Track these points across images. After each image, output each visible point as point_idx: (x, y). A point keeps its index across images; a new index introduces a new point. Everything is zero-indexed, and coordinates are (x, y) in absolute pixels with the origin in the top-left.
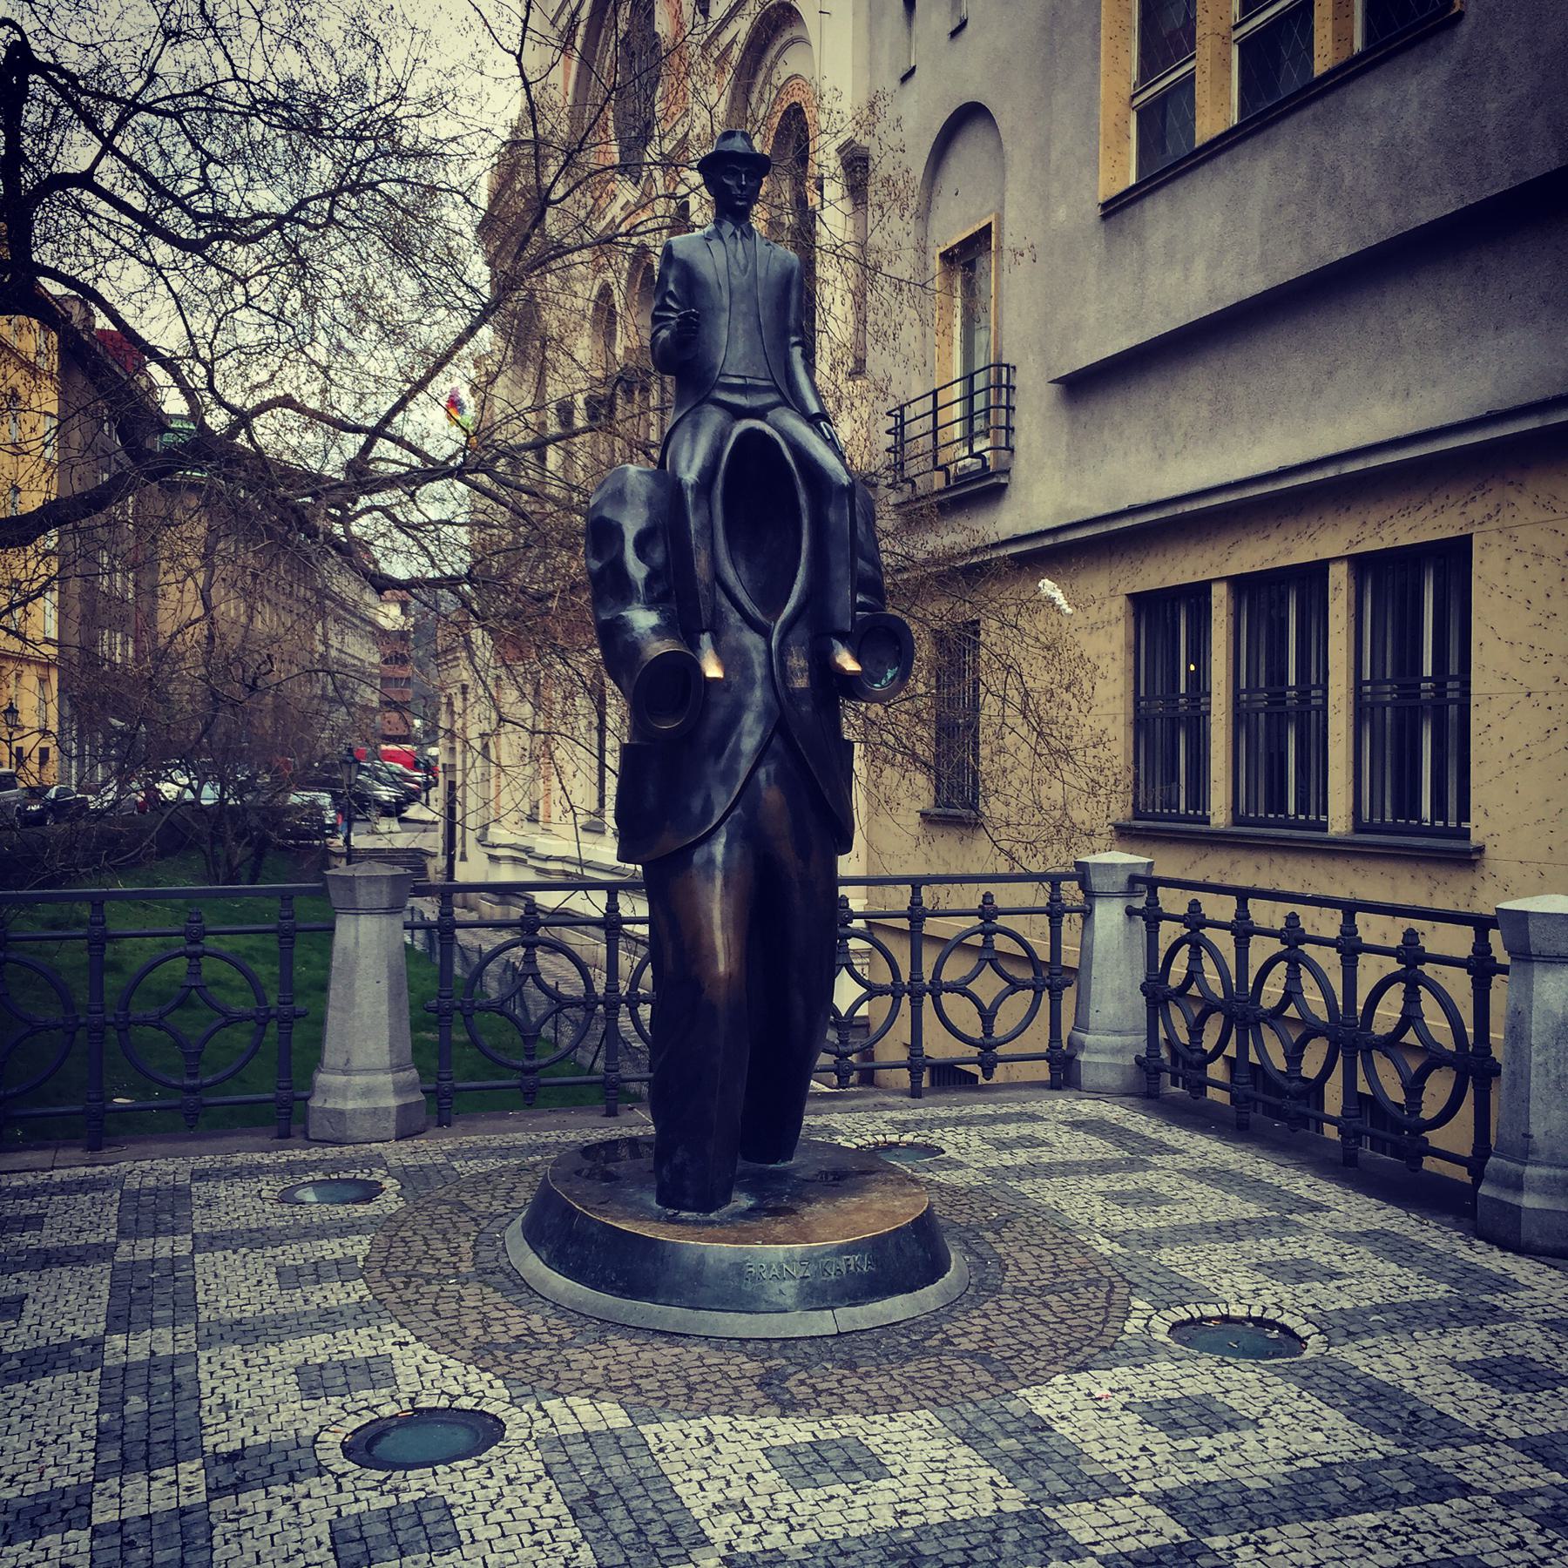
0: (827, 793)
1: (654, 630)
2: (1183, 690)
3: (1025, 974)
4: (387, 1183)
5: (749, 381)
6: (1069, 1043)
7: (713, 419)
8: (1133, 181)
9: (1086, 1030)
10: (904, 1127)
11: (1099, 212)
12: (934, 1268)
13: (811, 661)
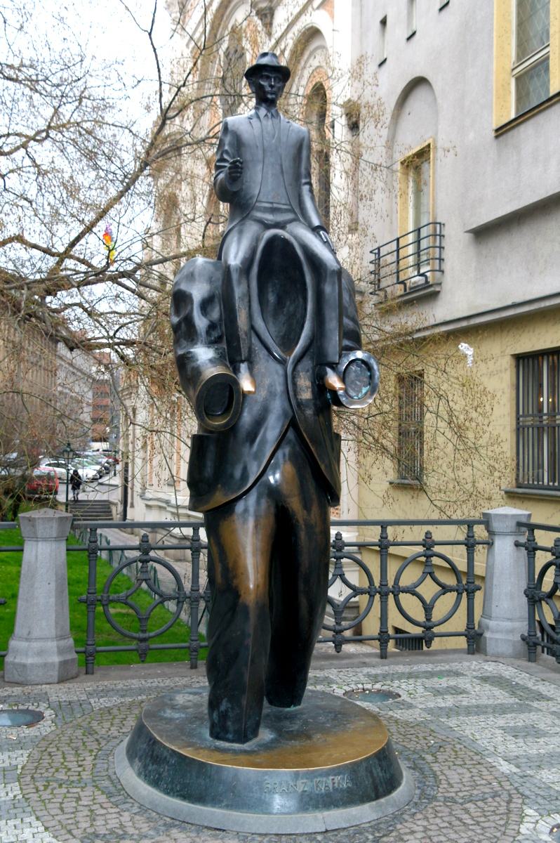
0: (323, 467)
1: (211, 361)
2: (545, 411)
3: (450, 580)
4: (48, 713)
5: (275, 205)
6: (479, 626)
7: (252, 229)
8: (513, 116)
9: (490, 618)
10: (375, 679)
11: (493, 134)
12: (391, 784)
13: (313, 383)
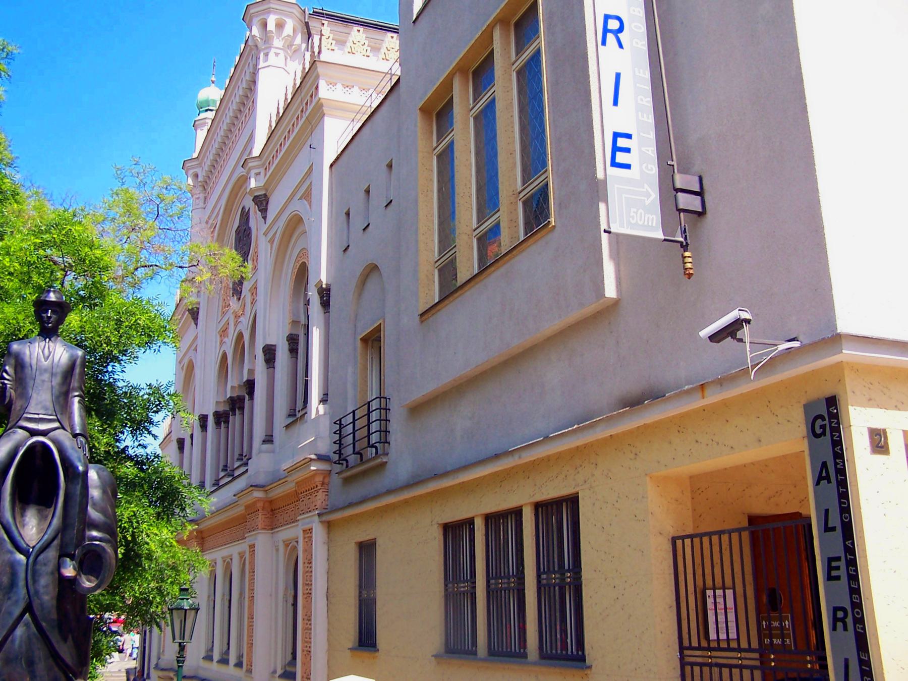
5: (41, 416)
